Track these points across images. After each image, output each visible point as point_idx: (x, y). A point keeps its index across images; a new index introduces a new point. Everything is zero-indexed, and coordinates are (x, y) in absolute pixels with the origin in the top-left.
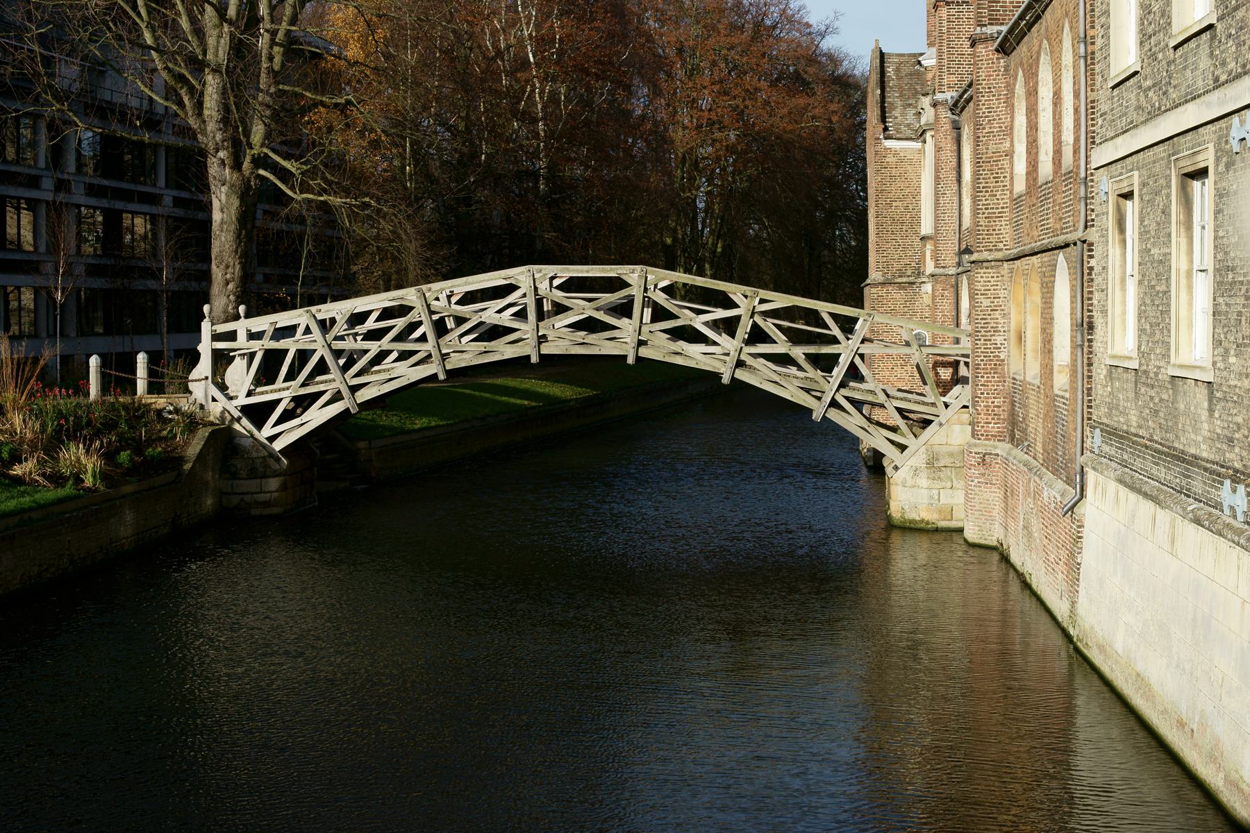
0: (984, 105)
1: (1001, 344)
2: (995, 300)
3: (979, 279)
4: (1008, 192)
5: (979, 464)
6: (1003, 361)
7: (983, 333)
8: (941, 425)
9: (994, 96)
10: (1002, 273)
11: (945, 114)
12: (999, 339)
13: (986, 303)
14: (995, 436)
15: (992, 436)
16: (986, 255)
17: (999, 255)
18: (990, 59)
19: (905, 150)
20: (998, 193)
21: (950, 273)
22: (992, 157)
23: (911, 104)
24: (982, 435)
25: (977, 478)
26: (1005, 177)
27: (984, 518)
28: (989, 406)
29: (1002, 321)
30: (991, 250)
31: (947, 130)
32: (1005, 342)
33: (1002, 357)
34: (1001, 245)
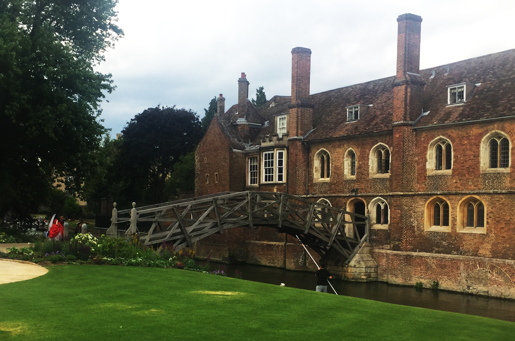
0: (406, 145)
1: (413, 221)
2: (411, 208)
3: (404, 200)
4: (416, 174)
5: (405, 259)
6: (414, 226)
7: (405, 218)
8: (360, 247)
9: (411, 143)
10: (414, 199)
11: (299, 144)
12: (412, 220)
13: (406, 208)
14: (410, 250)
15: (409, 250)
16: (406, 193)
17: (413, 193)
18: (409, 131)
19: (238, 153)
20: (412, 174)
21: (303, 197)
22: (409, 162)
23: (234, 137)
24: (404, 250)
25: (404, 263)
26: (414, 169)
27: (407, 276)
28: (408, 241)
29: (414, 214)
30: (408, 192)
31: (300, 149)
32: (415, 221)
33: (413, 225)
34: (413, 190)
